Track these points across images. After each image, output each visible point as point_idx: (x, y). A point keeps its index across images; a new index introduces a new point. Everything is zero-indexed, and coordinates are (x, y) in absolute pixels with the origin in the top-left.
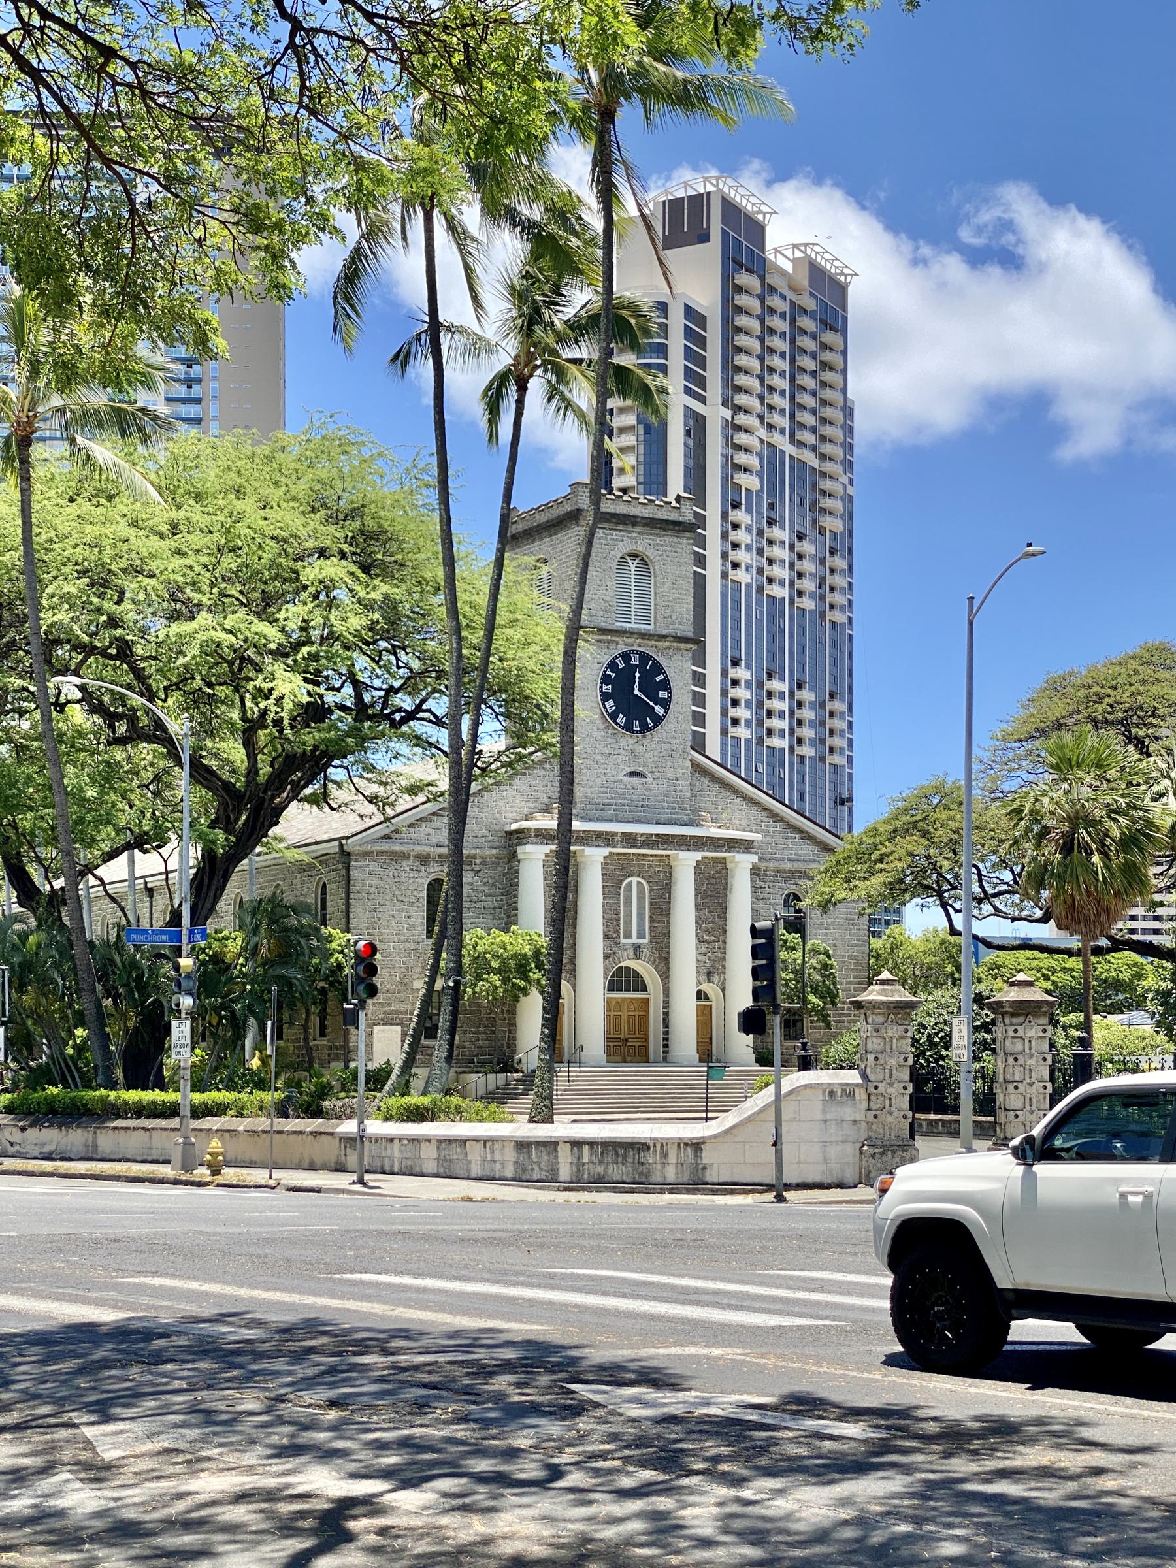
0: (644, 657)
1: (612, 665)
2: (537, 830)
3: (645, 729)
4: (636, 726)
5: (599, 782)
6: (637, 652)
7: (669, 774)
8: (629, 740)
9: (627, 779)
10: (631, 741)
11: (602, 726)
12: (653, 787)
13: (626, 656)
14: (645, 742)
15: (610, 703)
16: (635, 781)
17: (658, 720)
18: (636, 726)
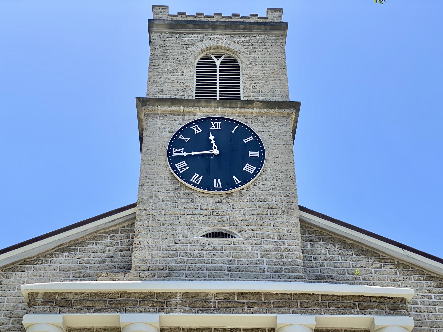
0: (228, 123)
1: (186, 130)
2: (45, 294)
3: (229, 185)
4: (218, 183)
5: (164, 244)
6: (219, 119)
7: (266, 231)
8: (209, 200)
9: (206, 238)
10: (211, 200)
11: (171, 187)
12: (243, 246)
13: (204, 123)
14: (232, 201)
15: (182, 166)
16: (217, 241)
17: (246, 178)
18: (218, 183)
